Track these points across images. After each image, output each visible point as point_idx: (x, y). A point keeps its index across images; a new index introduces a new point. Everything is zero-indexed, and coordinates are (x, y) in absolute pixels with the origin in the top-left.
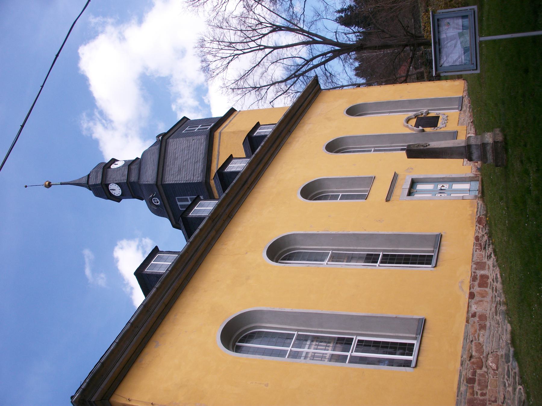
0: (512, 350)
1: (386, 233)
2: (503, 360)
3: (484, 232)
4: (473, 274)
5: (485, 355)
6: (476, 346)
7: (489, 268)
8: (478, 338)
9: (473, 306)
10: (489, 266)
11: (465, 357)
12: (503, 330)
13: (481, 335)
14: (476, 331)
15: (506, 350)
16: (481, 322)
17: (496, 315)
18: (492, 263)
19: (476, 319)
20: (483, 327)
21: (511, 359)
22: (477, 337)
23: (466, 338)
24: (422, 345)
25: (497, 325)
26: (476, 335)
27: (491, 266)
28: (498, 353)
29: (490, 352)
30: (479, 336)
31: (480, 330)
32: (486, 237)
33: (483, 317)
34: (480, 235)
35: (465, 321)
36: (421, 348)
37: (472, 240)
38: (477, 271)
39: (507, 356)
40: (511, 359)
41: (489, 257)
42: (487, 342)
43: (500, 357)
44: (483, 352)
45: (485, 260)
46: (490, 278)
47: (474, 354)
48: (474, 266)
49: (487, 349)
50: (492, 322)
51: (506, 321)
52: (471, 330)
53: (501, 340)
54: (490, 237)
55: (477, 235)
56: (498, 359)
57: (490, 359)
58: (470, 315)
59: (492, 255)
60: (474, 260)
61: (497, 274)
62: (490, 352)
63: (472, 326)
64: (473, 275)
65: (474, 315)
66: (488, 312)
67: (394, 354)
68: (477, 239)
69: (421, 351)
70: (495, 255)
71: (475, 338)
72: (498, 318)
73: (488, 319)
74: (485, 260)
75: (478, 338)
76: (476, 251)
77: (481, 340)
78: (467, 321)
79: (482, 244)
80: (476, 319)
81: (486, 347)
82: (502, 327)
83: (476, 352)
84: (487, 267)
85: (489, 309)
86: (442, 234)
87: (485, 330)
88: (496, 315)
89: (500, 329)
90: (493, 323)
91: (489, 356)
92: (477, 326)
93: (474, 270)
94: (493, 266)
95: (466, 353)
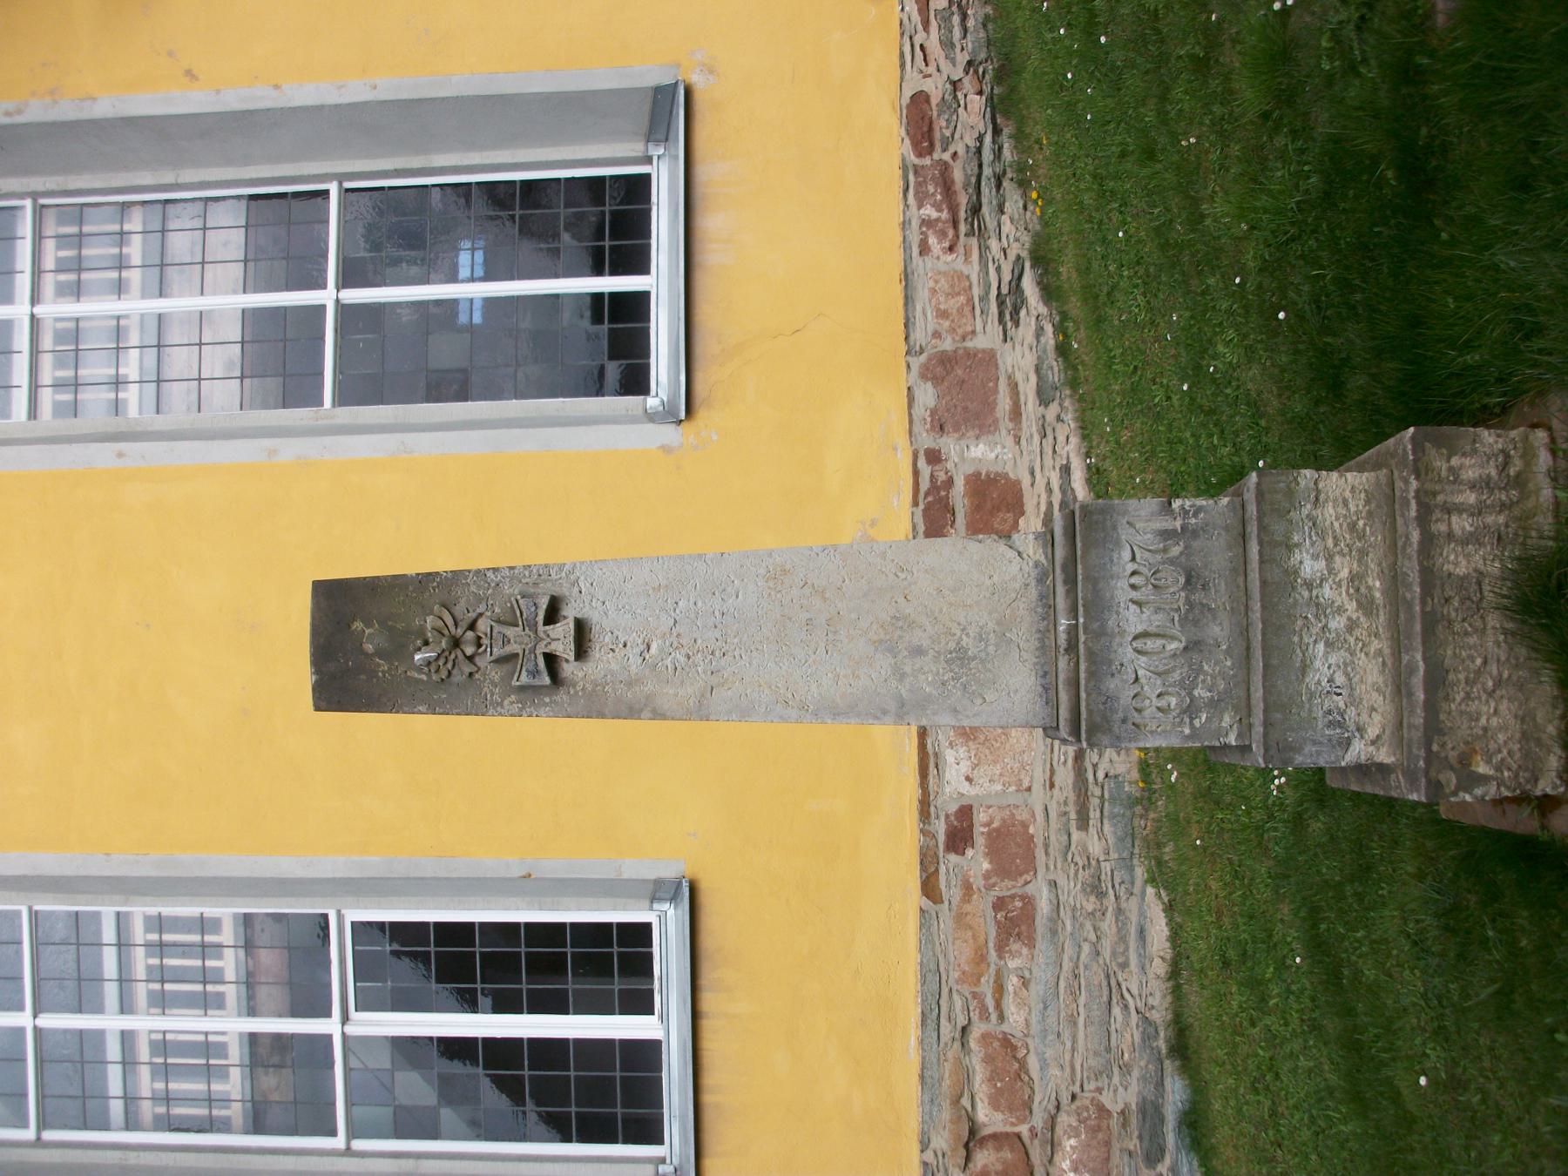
0: (1175, 1093)
1: (332, 98)
2: (1133, 1144)
3: (962, 58)
4: (925, 470)
5: (1038, 1120)
6: (988, 1060)
7: (1016, 414)
8: (998, 1006)
9: (949, 756)
10: (1014, 387)
11: (940, 1142)
12: (1122, 938)
13: (1012, 982)
14: (981, 958)
15: (1143, 1079)
16: (1004, 888)
17: (1083, 823)
18: (1029, 360)
19: (977, 862)
20: (1015, 923)
21: (1171, 1139)
22: (990, 1003)
23: (930, 1017)
24: (708, 1080)
25: (1090, 904)
26: (986, 987)
27: (1028, 389)
28: (1106, 1099)
29: (1065, 1099)
30: (999, 989)
31: (1001, 948)
32: (973, 112)
33: (1013, 849)
34: (935, 88)
35: (914, 883)
36: (707, 1098)
37: (890, 143)
38: (949, 445)
39: (1150, 1112)
40: (1171, 1139)
41: (1010, 306)
42: (1044, 1033)
43: (1115, 1122)
44: (1028, 1106)
45: (987, 337)
46: (1029, 505)
47: (983, 1113)
48: (927, 396)
49: (1048, 1079)
50: (1062, 882)
51: (1140, 873)
52: (959, 953)
53: (1117, 1011)
54: (998, 108)
55: (914, 84)
56: (1108, 1144)
57: (1070, 1143)
58: (940, 828)
59: (1029, 285)
60: (919, 336)
61: (1066, 470)
62: (1065, 1099)
63: (960, 919)
64: (925, 485)
65: (959, 838)
66: (1038, 798)
67: (425, 281)
68: (921, 122)
69: (708, 1116)
70: (1049, 293)
71: (984, 1011)
72: (1095, 848)
73: (1040, 853)
74: (987, 337)
75: (998, 1006)
76: (924, 249)
77: (1015, 1017)
78: (929, 888)
79: (958, 175)
80: (977, 862)
81: (1044, 1066)
82: (1119, 911)
83: (995, 1104)
84: (1004, 403)
85: (1039, 775)
86: (696, 79)
87: (1031, 944)
88: (1083, 823)
89: (1108, 925)
90: (1071, 890)
91: (1064, 1119)
92: (987, 925)
93: (927, 441)
94: (1044, 399)
95: (946, 1115)
